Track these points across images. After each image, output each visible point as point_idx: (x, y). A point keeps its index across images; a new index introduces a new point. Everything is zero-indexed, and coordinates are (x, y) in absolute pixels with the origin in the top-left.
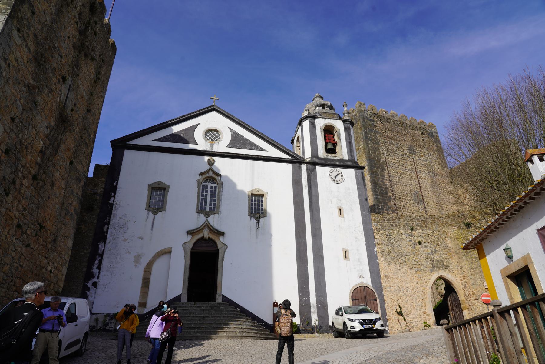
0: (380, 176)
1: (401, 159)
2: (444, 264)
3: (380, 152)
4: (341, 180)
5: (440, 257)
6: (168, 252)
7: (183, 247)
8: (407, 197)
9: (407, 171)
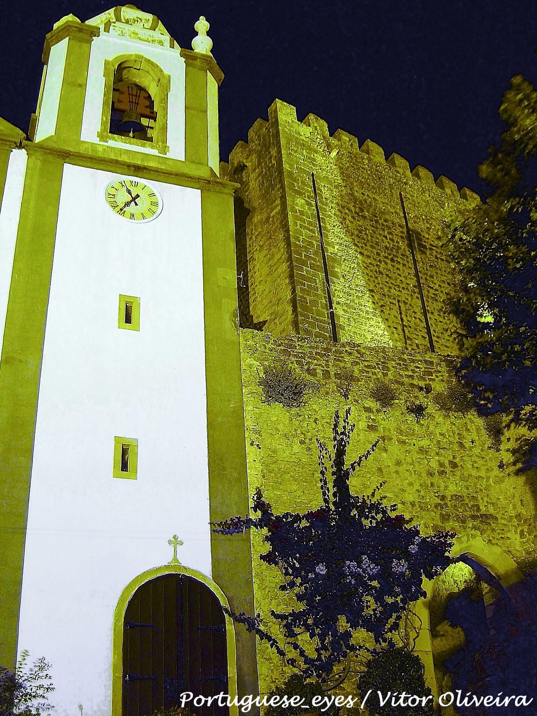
1: (386, 257)
2: (479, 509)
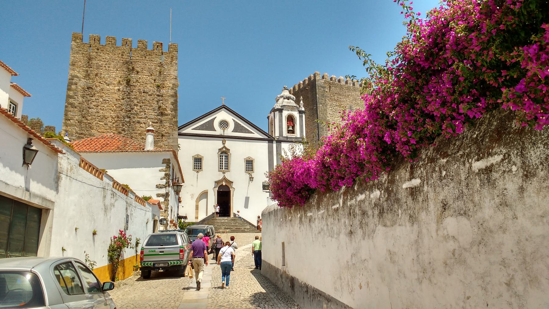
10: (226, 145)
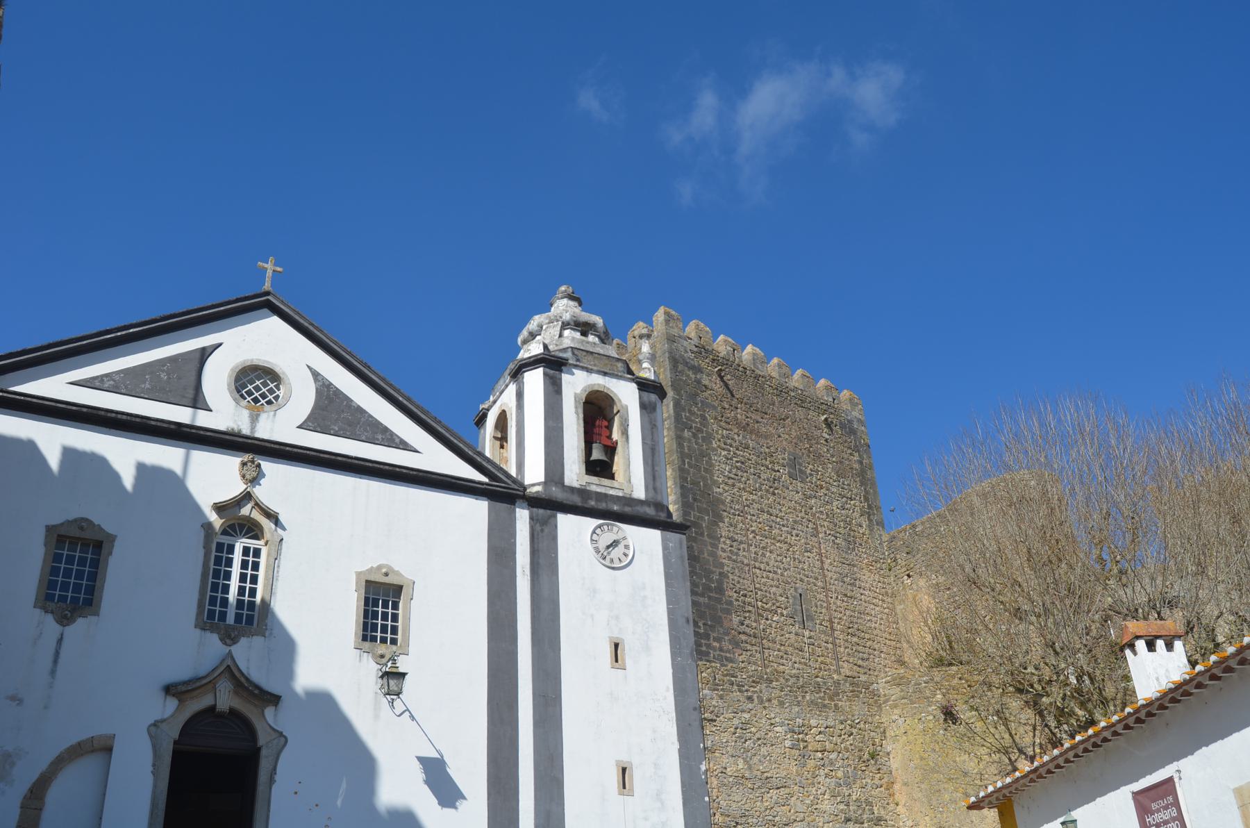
0: (706, 538)
3: (712, 465)
4: (623, 558)
5: (864, 793)
6: (103, 748)
7: (151, 736)
8: (774, 604)
9: (779, 529)
10: (260, 492)
